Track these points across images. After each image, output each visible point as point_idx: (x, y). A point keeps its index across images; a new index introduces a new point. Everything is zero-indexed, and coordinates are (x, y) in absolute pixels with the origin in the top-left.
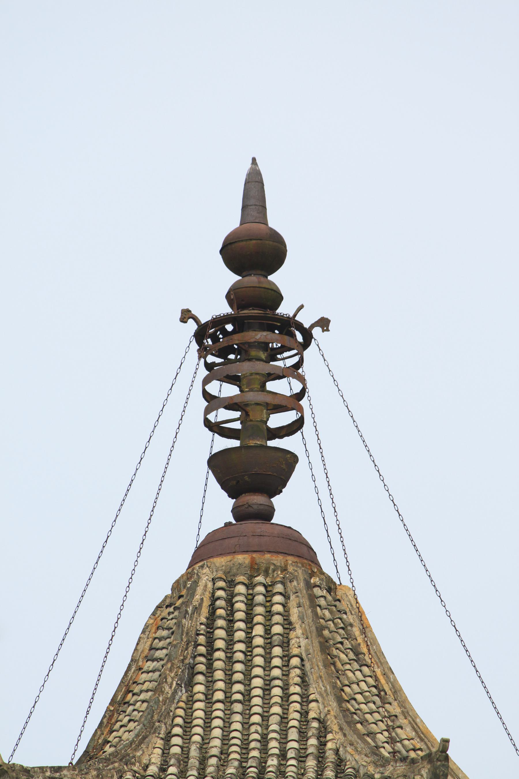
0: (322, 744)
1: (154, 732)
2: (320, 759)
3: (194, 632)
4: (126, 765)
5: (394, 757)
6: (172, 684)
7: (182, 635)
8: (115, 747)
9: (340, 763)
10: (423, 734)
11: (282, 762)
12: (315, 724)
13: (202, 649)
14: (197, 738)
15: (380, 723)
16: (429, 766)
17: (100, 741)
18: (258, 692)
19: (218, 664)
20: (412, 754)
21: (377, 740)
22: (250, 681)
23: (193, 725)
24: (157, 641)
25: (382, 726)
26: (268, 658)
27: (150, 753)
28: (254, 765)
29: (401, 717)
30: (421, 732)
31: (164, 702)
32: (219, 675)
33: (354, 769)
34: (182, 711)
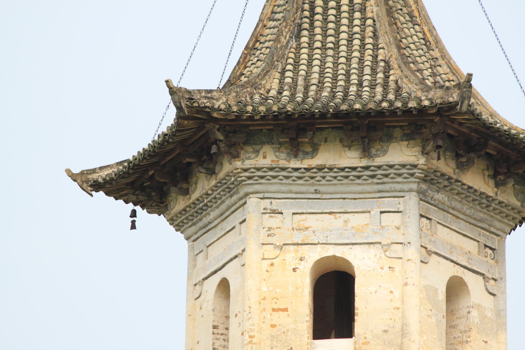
0: (387, 77)
1: (274, 68)
2: (385, 87)
3: (301, 2)
4: (255, 89)
5: (435, 85)
6: (286, 36)
7: (293, 3)
8: (248, 77)
9: (398, 90)
10: (455, 70)
11: (360, 89)
12: (382, 64)
13: (307, 13)
14: (302, 73)
15: (426, 63)
16: (458, 92)
17: (238, 74)
18: (344, 42)
19: (317, 24)
20: (447, 84)
21: (424, 75)
22: (339, 34)
23: (300, 63)
24: (276, 7)
25: (427, 65)
26: (351, 20)
27: (271, 82)
28: (341, 90)
29: (440, 59)
30: (453, 69)
31: (281, 48)
32: (318, 30)
33: (408, 93)
34: (293, 54)
